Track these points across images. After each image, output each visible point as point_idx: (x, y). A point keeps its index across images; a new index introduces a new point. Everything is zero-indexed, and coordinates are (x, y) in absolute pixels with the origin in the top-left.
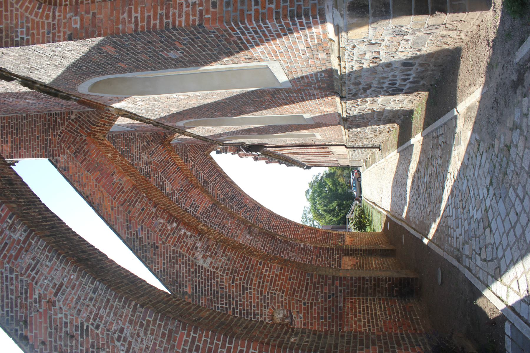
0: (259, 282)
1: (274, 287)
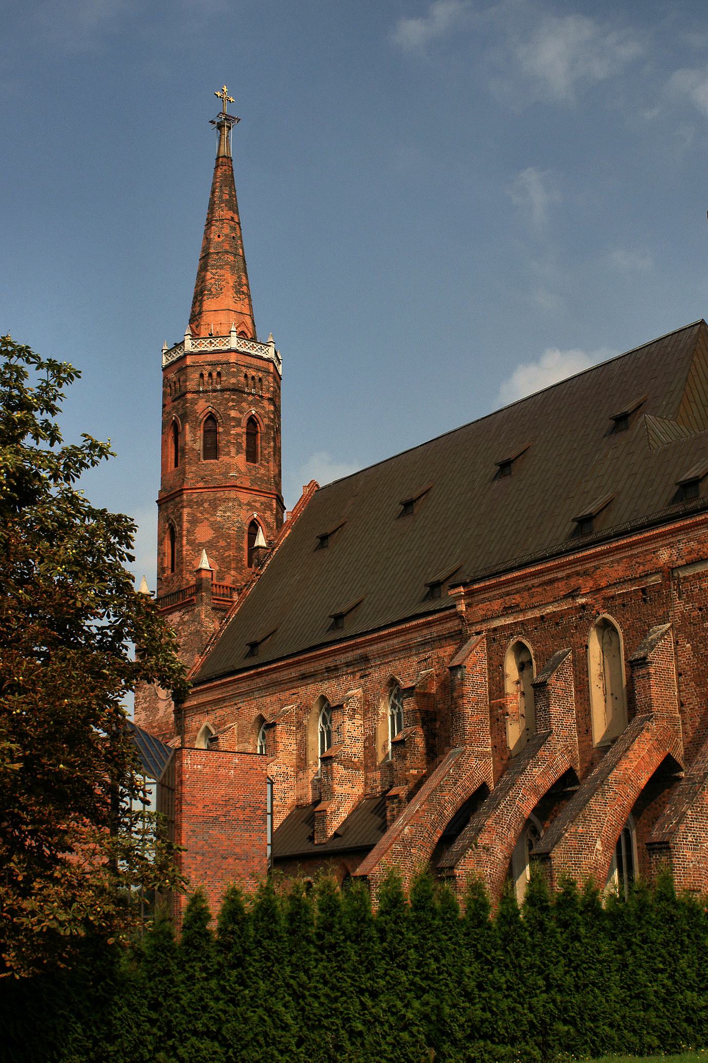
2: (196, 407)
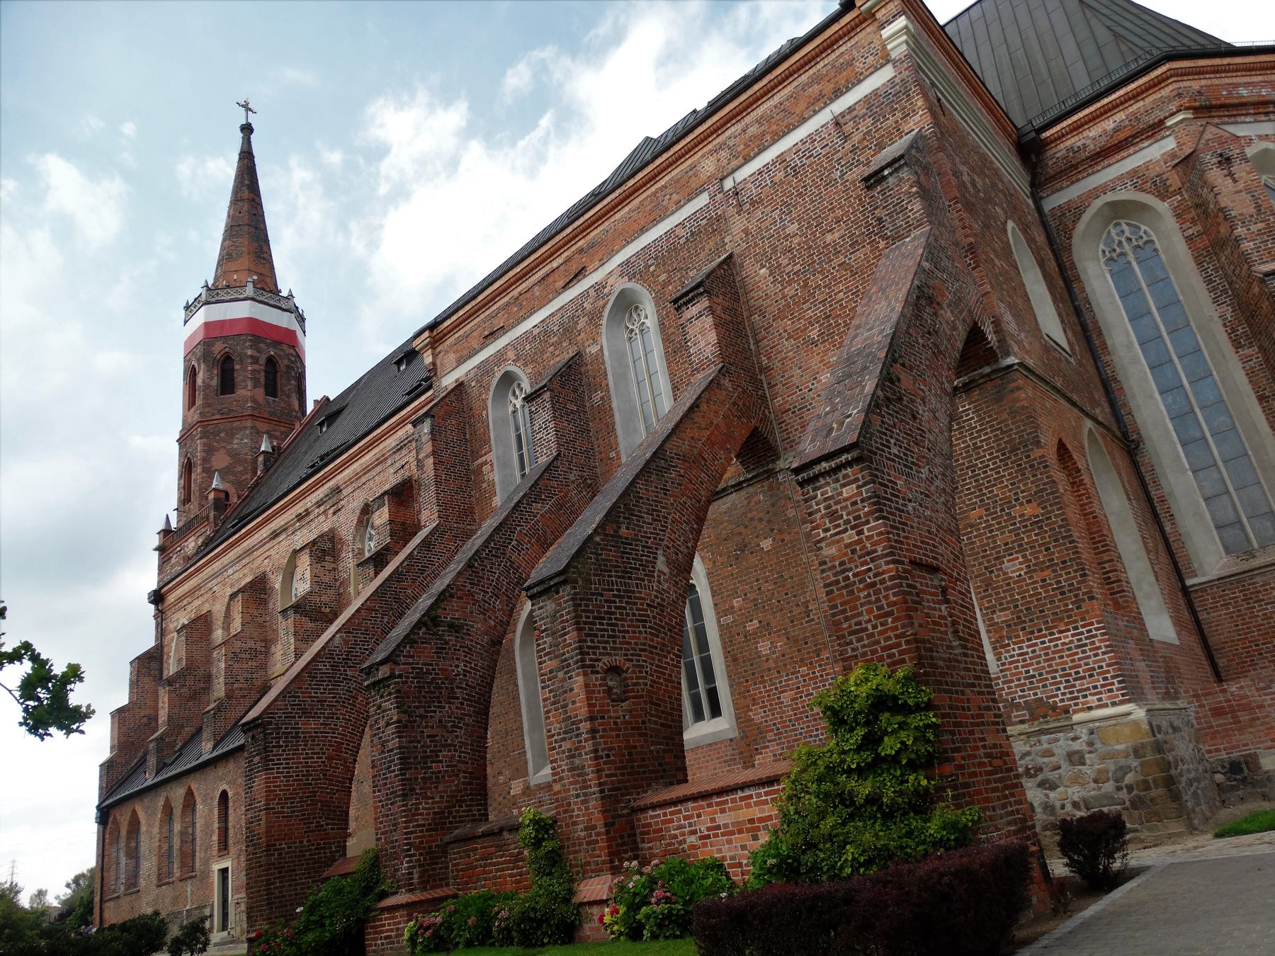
0: (656, 648)
1: (656, 671)
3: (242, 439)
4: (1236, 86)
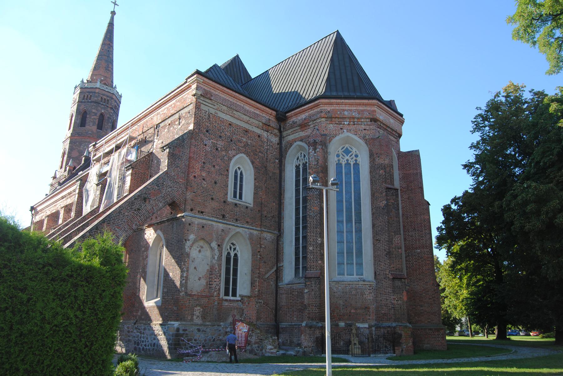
2: (80, 107)
3: (84, 146)
4: (344, 110)
